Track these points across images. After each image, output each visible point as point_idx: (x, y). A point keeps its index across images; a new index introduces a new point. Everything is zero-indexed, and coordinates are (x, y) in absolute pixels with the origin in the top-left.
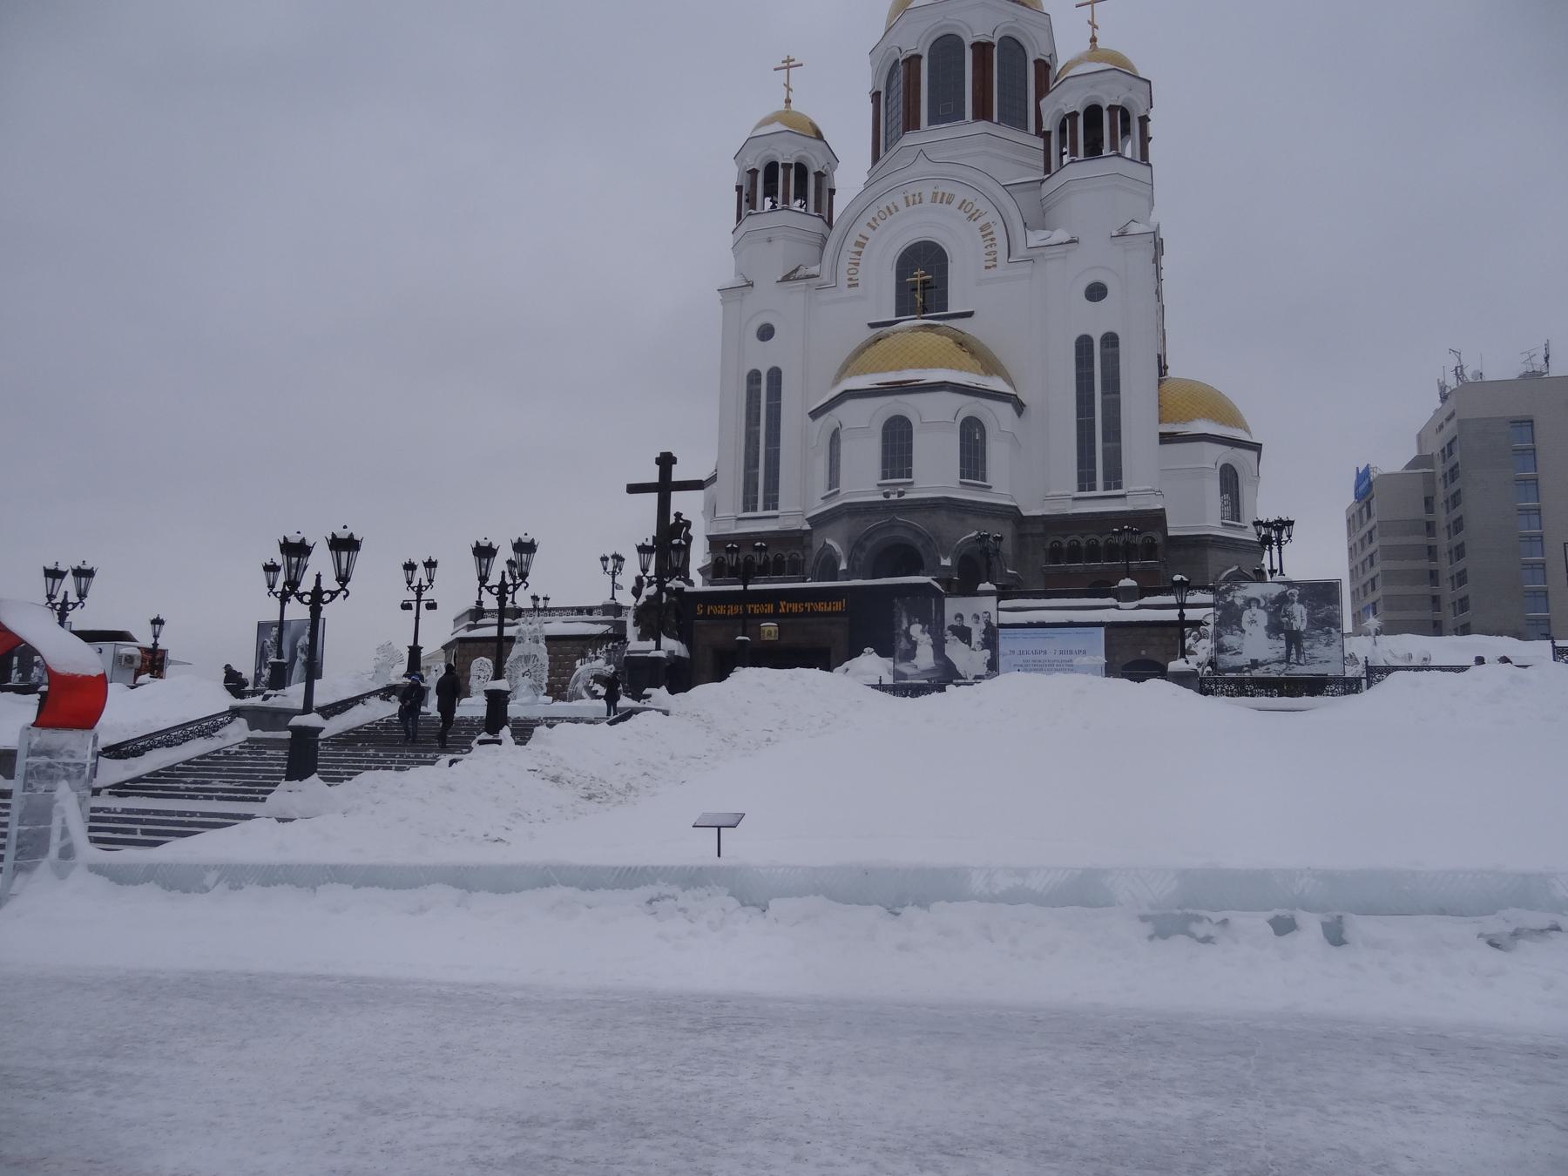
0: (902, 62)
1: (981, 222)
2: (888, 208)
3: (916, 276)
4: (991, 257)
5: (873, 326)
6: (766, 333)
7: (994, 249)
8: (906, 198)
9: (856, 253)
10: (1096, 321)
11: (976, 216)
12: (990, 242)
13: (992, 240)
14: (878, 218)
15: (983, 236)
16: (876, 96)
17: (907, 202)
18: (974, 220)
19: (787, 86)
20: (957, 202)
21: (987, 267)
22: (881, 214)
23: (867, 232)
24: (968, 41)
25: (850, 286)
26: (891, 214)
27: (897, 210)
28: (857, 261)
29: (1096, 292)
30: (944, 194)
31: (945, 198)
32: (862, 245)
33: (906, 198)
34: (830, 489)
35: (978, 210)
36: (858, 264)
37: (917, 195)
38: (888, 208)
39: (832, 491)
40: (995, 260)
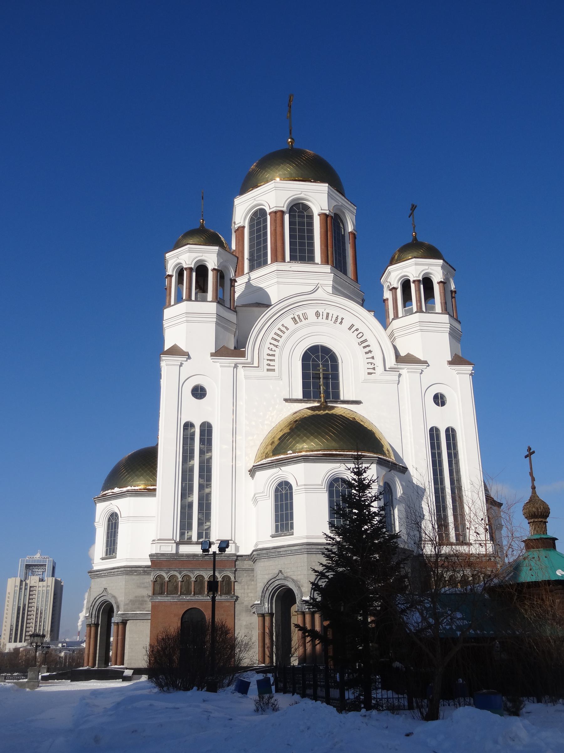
4: (372, 366)
21: (369, 374)
25: (268, 370)
40: (374, 369)
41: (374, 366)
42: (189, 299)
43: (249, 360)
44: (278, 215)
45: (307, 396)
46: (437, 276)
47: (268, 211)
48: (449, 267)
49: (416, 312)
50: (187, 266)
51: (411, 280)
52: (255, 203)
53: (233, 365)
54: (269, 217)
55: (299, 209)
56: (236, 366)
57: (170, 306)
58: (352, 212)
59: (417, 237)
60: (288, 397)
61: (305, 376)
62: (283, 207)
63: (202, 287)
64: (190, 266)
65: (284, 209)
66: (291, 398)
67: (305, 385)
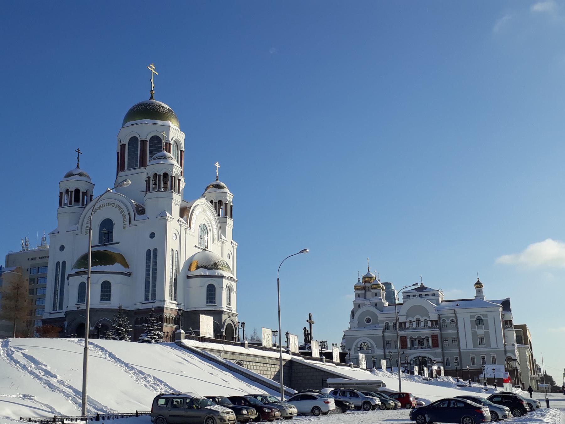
3: (103, 231)
6: (62, 248)
10: (151, 245)
16: (118, 153)
24: (139, 140)
29: (152, 235)
34: (78, 303)
39: (78, 304)
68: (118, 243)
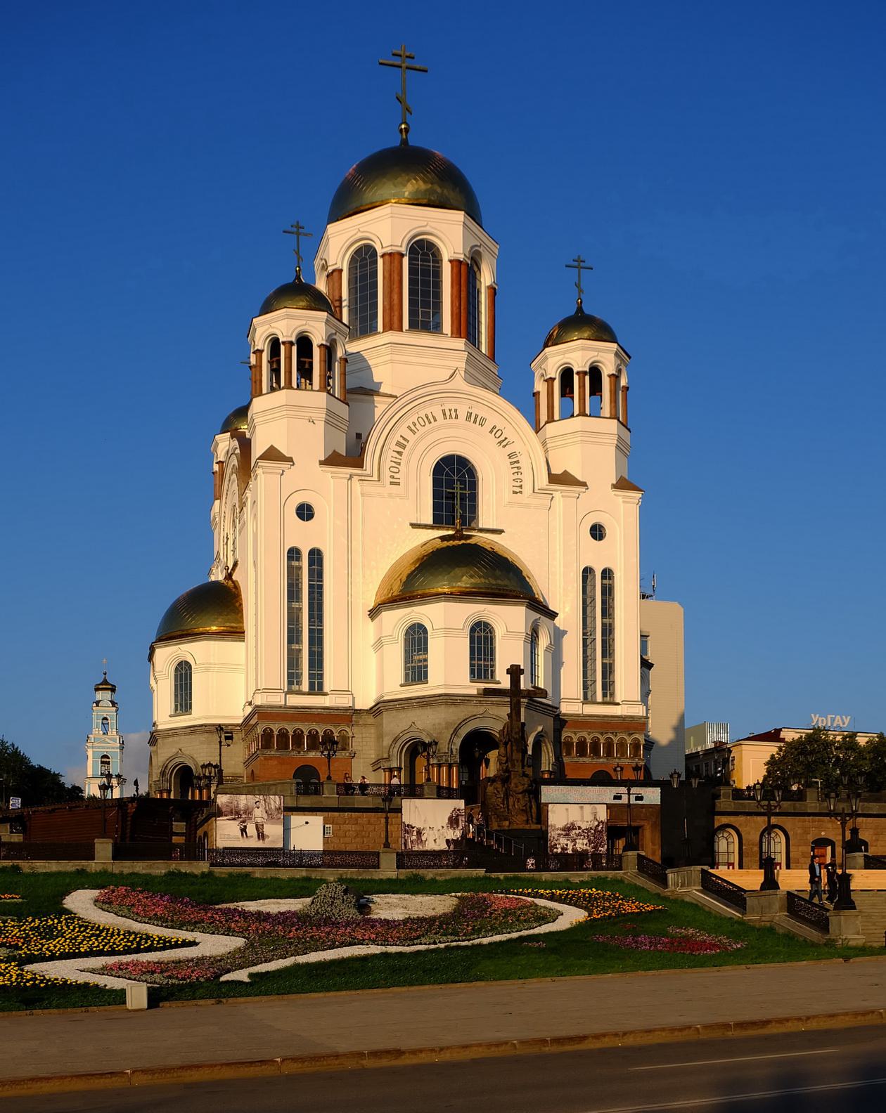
0: (383, 256)
1: (509, 450)
2: (427, 416)
4: (518, 484)
5: (414, 526)
7: (519, 476)
8: (444, 411)
9: (398, 452)
11: (504, 443)
12: (516, 470)
13: (518, 468)
14: (417, 423)
15: (512, 463)
17: (445, 415)
18: (505, 446)
19: (297, 253)
20: (488, 426)
21: (515, 493)
22: (420, 419)
23: (408, 435)
25: (391, 483)
26: (430, 423)
27: (435, 420)
28: (399, 461)
30: (476, 416)
31: (478, 420)
32: (404, 447)
33: (444, 411)
35: (506, 438)
36: (399, 464)
37: (453, 410)
38: (427, 416)
40: (521, 486)
41: (521, 484)
42: (289, 386)
43: (368, 472)
44: (394, 257)
45: (438, 521)
46: (608, 369)
47: (380, 252)
48: (624, 354)
49: (577, 416)
50: (285, 339)
51: (575, 372)
52: (360, 235)
53: (348, 476)
54: (380, 261)
55: (422, 249)
56: (351, 478)
57: (261, 394)
58: (491, 252)
59: (583, 308)
60: (414, 522)
61: (437, 495)
62: (401, 246)
63: (305, 371)
64: (290, 339)
65: (403, 250)
66: (419, 522)
67: (437, 507)
68: (500, 532)
